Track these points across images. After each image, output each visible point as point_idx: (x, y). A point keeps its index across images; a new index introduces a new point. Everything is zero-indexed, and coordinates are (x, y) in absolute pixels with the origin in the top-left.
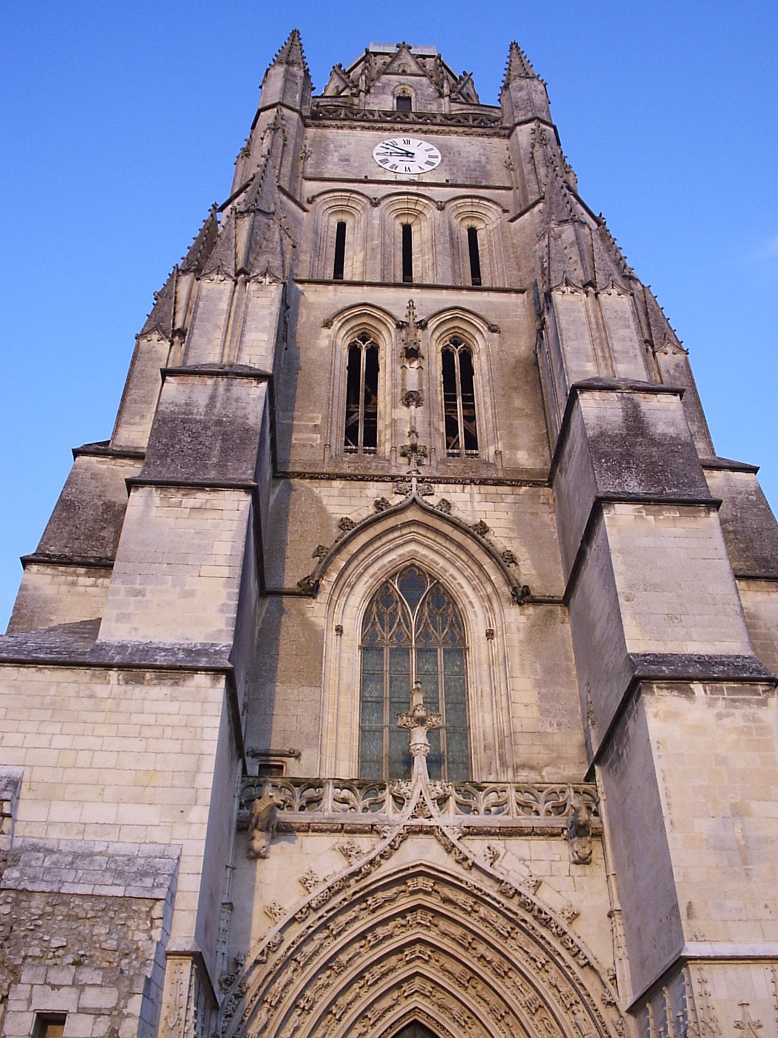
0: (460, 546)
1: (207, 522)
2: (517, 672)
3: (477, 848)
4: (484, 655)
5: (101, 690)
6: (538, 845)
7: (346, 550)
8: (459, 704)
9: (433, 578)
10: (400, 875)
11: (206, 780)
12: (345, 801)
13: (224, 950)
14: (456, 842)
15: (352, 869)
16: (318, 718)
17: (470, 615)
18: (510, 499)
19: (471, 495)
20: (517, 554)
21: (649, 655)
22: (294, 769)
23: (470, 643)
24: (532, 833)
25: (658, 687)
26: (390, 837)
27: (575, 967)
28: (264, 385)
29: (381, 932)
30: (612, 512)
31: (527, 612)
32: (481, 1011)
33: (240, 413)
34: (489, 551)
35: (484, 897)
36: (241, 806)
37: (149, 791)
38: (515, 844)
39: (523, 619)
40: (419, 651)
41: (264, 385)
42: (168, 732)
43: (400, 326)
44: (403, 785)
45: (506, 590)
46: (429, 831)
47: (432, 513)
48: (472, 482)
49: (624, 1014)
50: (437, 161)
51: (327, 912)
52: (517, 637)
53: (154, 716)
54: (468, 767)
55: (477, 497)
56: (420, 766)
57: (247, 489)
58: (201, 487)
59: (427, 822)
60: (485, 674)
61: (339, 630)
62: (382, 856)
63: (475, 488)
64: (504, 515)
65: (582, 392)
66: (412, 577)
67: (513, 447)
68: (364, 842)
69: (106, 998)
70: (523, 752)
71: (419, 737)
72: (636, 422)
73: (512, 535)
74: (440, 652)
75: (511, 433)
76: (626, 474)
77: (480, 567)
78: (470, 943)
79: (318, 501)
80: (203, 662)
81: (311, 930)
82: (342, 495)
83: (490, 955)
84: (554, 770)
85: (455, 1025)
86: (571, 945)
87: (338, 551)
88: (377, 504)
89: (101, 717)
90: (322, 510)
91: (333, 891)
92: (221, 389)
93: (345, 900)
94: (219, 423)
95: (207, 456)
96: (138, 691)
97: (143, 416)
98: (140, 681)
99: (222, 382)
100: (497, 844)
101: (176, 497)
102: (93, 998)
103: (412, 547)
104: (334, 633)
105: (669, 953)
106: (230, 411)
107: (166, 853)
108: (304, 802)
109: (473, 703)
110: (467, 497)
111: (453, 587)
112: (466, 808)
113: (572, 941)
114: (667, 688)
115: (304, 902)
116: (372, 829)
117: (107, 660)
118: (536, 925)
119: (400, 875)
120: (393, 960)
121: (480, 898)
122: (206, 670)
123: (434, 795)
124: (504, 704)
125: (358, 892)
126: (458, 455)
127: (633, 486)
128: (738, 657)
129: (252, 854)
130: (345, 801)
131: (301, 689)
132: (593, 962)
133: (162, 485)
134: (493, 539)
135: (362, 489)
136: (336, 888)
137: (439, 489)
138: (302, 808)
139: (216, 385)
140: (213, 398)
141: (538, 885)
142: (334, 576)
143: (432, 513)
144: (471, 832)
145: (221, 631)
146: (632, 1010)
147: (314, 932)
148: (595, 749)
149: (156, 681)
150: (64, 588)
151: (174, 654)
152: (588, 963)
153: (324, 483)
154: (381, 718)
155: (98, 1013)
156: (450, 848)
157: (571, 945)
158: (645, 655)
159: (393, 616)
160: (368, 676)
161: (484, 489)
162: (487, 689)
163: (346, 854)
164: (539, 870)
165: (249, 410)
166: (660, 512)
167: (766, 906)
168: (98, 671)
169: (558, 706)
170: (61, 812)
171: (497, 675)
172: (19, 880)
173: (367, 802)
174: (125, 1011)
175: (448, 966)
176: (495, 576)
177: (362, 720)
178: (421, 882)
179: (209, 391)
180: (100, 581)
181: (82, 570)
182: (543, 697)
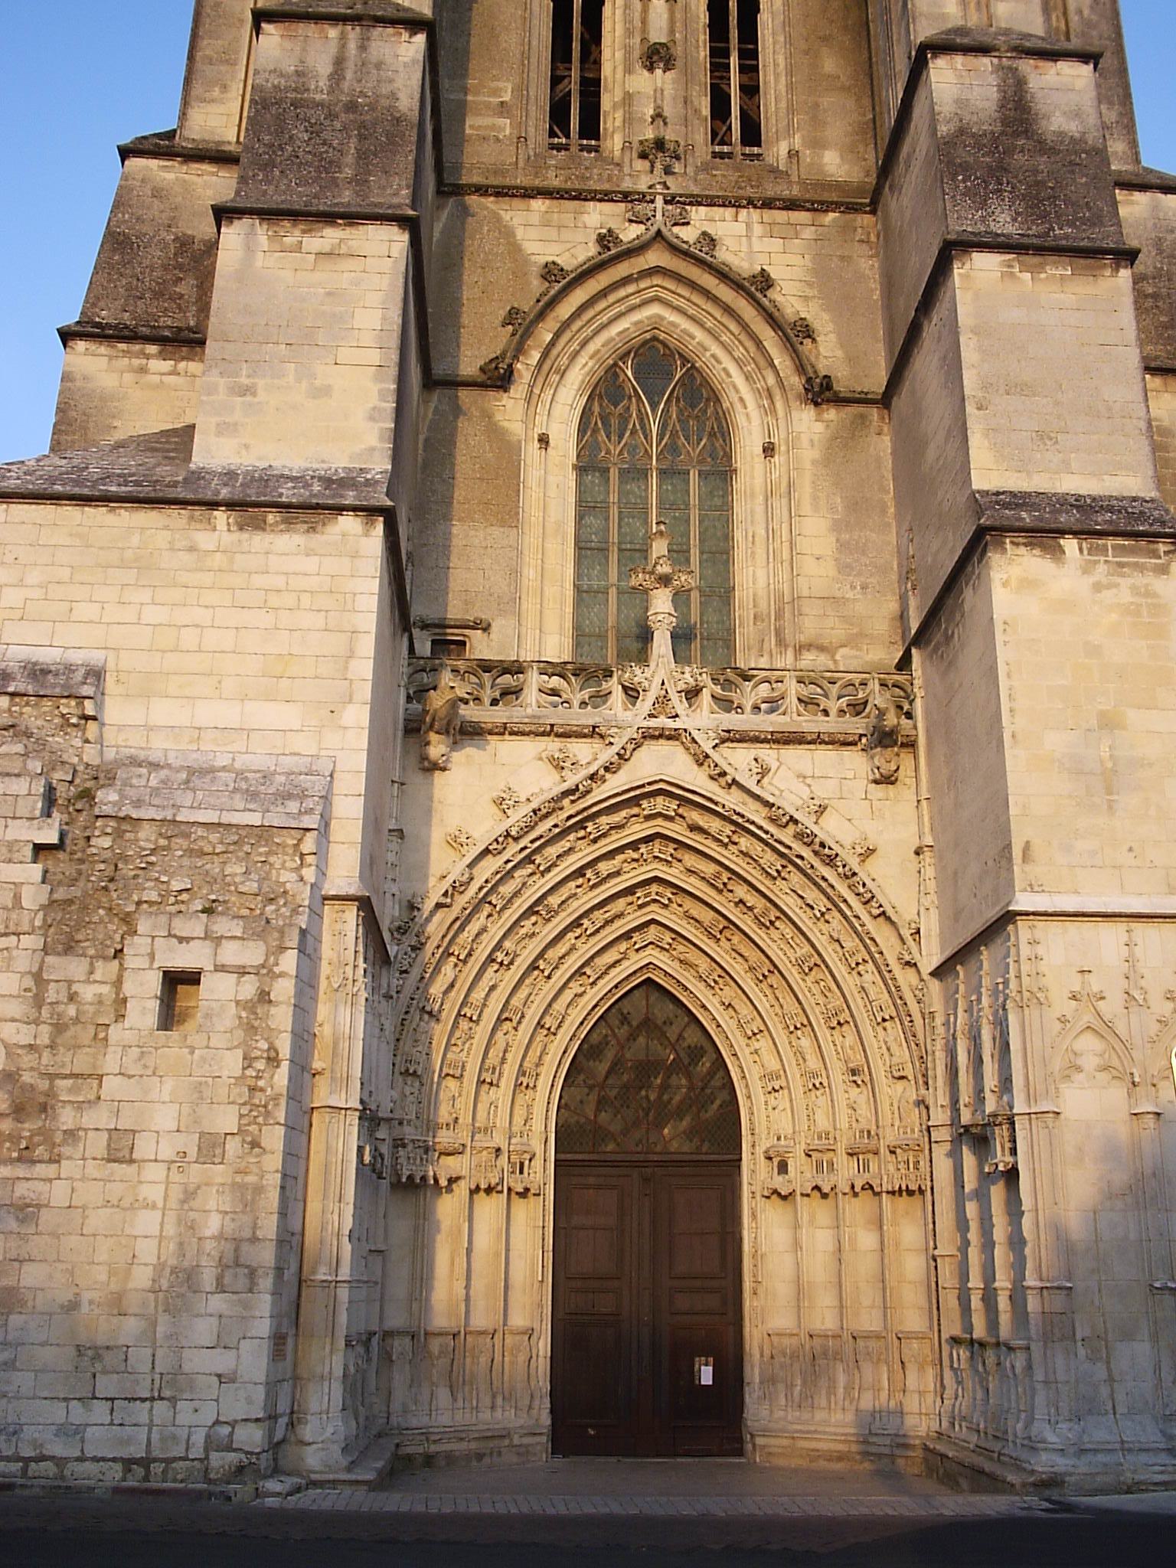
0: (728, 310)
1: (343, 275)
2: (806, 508)
3: (739, 760)
4: (759, 482)
5: (205, 539)
6: (824, 757)
7: (553, 314)
8: (720, 553)
9: (685, 360)
10: (632, 794)
11: (364, 668)
12: (554, 692)
13: (395, 890)
14: (710, 752)
15: (565, 786)
16: (515, 573)
17: (740, 419)
18: (808, 233)
19: (748, 225)
20: (816, 325)
21: (1003, 493)
22: (481, 647)
23: (739, 462)
24: (818, 740)
25: (1012, 542)
26: (619, 743)
27: (865, 918)
28: (421, 39)
29: (604, 867)
30: (967, 266)
31: (826, 416)
32: (737, 969)
33: (385, 90)
34: (772, 319)
35: (747, 825)
36: (409, 699)
37: (284, 682)
38: (793, 755)
39: (819, 427)
40: (662, 473)
41: (421, 39)
42: (306, 600)
44: (638, 671)
45: (796, 382)
46: (673, 736)
47: (686, 254)
48: (751, 203)
49: (926, 977)
51: (532, 842)
52: (809, 454)
53: (283, 578)
54: (729, 644)
55: (758, 230)
56: (662, 644)
57: (402, 221)
58: (329, 218)
59: (671, 724)
60: (760, 509)
61: (544, 440)
62: (607, 769)
63: (755, 214)
64: (797, 260)
65: (935, 56)
66: (654, 359)
67: (817, 144)
68: (583, 751)
69: (253, 954)
70: (809, 628)
71: (661, 603)
72: (1017, 110)
73: (810, 292)
74: (694, 476)
75: (816, 120)
76: (993, 202)
77: (759, 344)
78: (725, 884)
79: (508, 233)
80: (350, 498)
81: (510, 865)
82: (546, 224)
83: (751, 899)
84: (854, 652)
85: (702, 985)
86: (862, 890)
87: (541, 315)
88: (601, 239)
89: (207, 578)
90: (515, 249)
91: (539, 815)
92: (352, 46)
93: (556, 826)
94: (352, 107)
95: (334, 165)
96: (258, 540)
97: (225, 88)
98: (260, 526)
99: (353, 33)
100: (768, 754)
101: (292, 234)
102: (231, 954)
103: (655, 309)
104: (537, 445)
105: (994, 905)
106: (368, 86)
107: (314, 768)
108: (497, 694)
109: (740, 554)
110: (740, 228)
111: (716, 375)
112: (726, 704)
113: (864, 885)
114: (1025, 545)
115: (501, 829)
116: (594, 732)
117: (209, 496)
118: (816, 863)
119: (632, 794)
120: (620, 904)
121: (740, 825)
122: (355, 509)
123: (681, 686)
124: (786, 555)
125: (574, 815)
126: (730, 155)
127: (1004, 223)
128: (1134, 499)
129: (426, 764)
130: (554, 692)
131: (489, 530)
132: (890, 912)
133: (269, 214)
134: (779, 298)
135: (578, 213)
136: (544, 811)
137: (699, 215)
138: (494, 702)
139: (343, 37)
140: (339, 62)
141: (822, 810)
142: (535, 356)
143: (686, 254)
144: (732, 737)
145: (373, 449)
146: (936, 973)
147: (515, 867)
148: (914, 626)
149: (282, 527)
150: (128, 377)
151: (307, 486)
152: (884, 913)
153: (517, 203)
154: (606, 573)
155: (242, 972)
156: (702, 759)
157: (862, 890)
158: (998, 494)
159: (624, 419)
160: (586, 507)
161: (770, 215)
162: (761, 532)
163: (558, 765)
164: (824, 791)
165: (399, 83)
166: (1041, 268)
167: (1130, 849)
168: (198, 512)
169: (865, 560)
170: (163, 712)
171: (777, 512)
172: (118, 804)
173: (585, 694)
174: (276, 970)
175: (694, 913)
176: (781, 360)
177: (578, 575)
178: (660, 804)
179: (332, 49)
180: (182, 365)
181: (152, 349)
182: (842, 546)
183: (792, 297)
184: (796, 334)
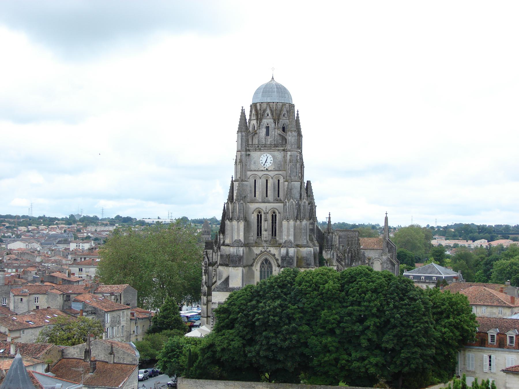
43: (264, 213)
50: (272, 162)
183: (277, 257)
184: (277, 260)
